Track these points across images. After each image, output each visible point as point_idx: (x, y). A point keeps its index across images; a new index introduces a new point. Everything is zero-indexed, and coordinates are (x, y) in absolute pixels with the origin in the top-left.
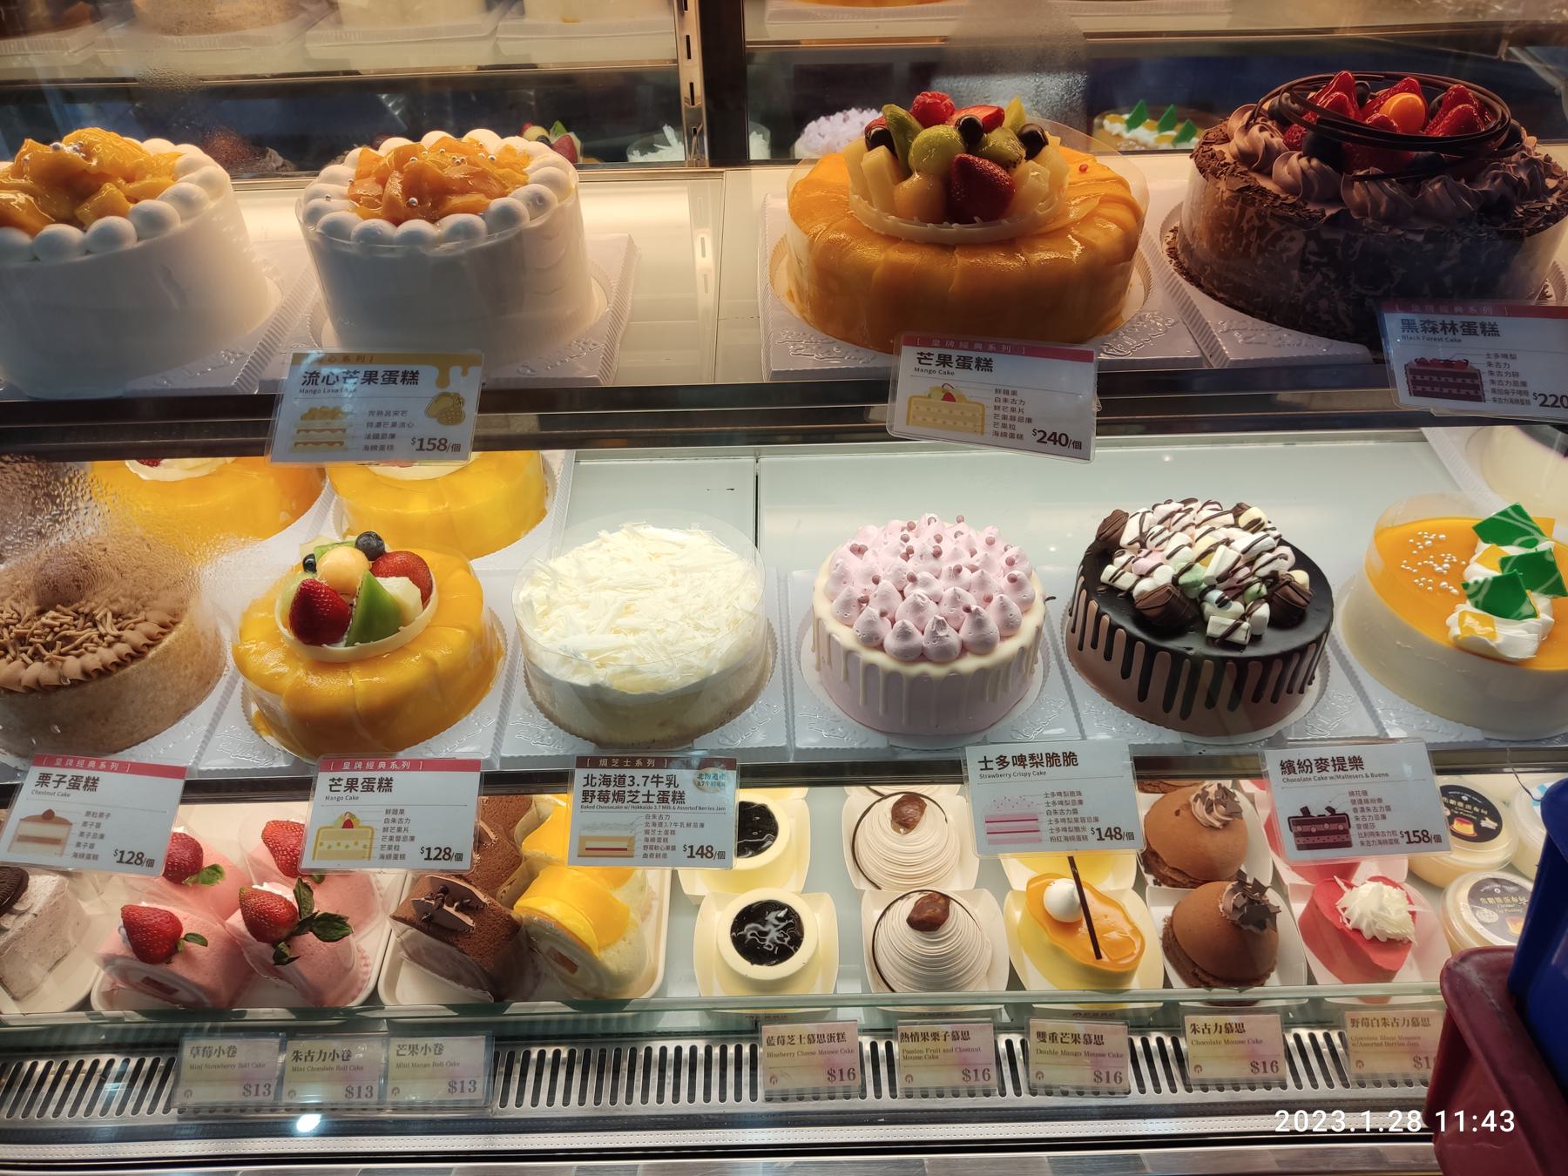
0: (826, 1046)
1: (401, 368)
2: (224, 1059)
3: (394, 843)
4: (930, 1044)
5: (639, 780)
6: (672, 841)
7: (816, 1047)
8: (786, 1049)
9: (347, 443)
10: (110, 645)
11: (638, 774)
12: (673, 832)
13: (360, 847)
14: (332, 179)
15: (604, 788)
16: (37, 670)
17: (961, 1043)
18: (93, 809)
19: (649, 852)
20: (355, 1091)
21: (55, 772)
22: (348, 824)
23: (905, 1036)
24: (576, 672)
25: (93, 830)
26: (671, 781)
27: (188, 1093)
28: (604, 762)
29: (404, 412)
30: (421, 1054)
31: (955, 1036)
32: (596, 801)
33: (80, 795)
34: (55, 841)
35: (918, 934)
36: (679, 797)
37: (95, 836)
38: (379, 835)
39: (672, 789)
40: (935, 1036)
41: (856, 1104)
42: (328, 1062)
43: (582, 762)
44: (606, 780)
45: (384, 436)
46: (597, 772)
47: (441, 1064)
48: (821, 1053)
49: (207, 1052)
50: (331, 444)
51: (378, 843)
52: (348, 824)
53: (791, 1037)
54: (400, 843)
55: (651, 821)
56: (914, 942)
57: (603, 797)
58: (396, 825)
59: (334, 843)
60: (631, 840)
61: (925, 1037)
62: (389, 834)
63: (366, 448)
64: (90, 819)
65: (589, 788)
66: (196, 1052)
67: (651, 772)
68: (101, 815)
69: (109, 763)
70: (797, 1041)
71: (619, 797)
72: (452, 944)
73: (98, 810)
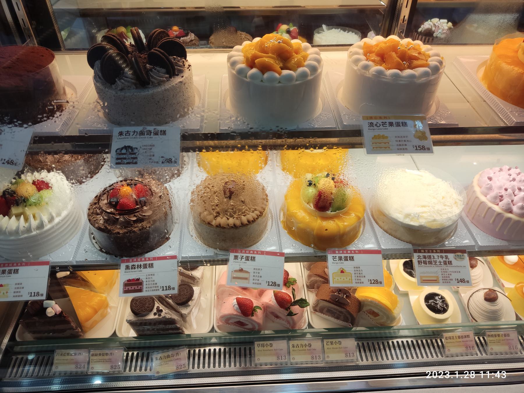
0: (465, 339)
1: (401, 121)
2: (269, 348)
3: (359, 278)
4: (497, 338)
5: (436, 257)
6: (451, 277)
7: (461, 340)
8: (452, 340)
9: (391, 147)
10: (253, 212)
11: (436, 255)
12: (451, 274)
13: (348, 280)
14: (238, 51)
15: (424, 260)
16: (231, 221)
17: (507, 338)
18: (256, 268)
19: (444, 281)
20: (315, 357)
21: (239, 255)
22: (342, 272)
23: (489, 336)
24: (411, 221)
25: (257, 275)
26: (446, 257)
27: (57, 367)
28: (422, 251)
29: (407, 137)
30: (334, 345)
31: (505, 335)
32: (423, 264)
33: (250, 262)
34: (246, 279)
35: (488, 303)
36: (450, 263)
37: (258, 276)
38: (353, 275)
39: (447, 260)
40: (499, 335)
41: (517, 356)
42: (304, 348)
43: (415, 251)
44: (425, 257)
45: (403, 145)
46: (421, 254)
47: (341, 348)
48: (463, 341)
49: (263, 346)
50: (386, 148)
51: (354, 278)
52: (342, 272)
53: (453, 337)
54: (361, 278)
55: (443, 271)
56: (487, 306)
57: (425, 263)
58: (358, 272)
59: (339, 278)
60: (437, 277)
61: (495, 336)
62: (356, 275)
63: (398, 149)
64: (255, 271)
65: (419, 260)
66: (259, 345)
67: (439, 254)
68: (259, 269)
69: (245, 251)
70: (455, 338)
71: (430, 263)
72: (344, 308)
73: (258, 268)
